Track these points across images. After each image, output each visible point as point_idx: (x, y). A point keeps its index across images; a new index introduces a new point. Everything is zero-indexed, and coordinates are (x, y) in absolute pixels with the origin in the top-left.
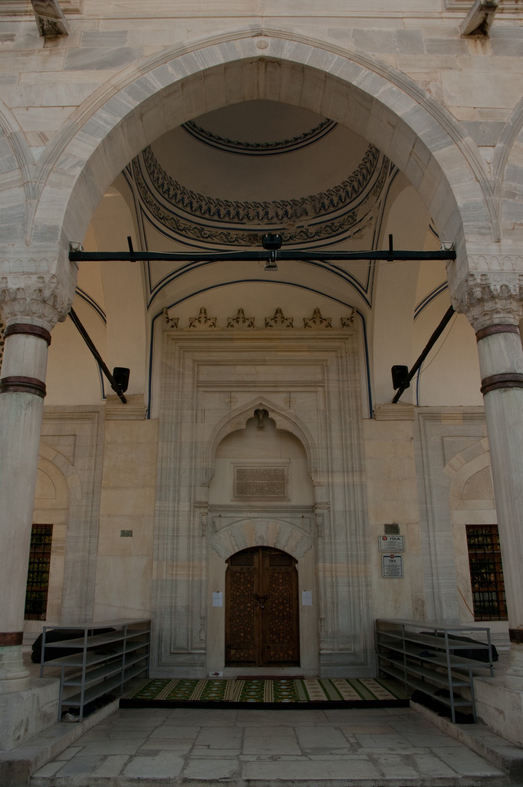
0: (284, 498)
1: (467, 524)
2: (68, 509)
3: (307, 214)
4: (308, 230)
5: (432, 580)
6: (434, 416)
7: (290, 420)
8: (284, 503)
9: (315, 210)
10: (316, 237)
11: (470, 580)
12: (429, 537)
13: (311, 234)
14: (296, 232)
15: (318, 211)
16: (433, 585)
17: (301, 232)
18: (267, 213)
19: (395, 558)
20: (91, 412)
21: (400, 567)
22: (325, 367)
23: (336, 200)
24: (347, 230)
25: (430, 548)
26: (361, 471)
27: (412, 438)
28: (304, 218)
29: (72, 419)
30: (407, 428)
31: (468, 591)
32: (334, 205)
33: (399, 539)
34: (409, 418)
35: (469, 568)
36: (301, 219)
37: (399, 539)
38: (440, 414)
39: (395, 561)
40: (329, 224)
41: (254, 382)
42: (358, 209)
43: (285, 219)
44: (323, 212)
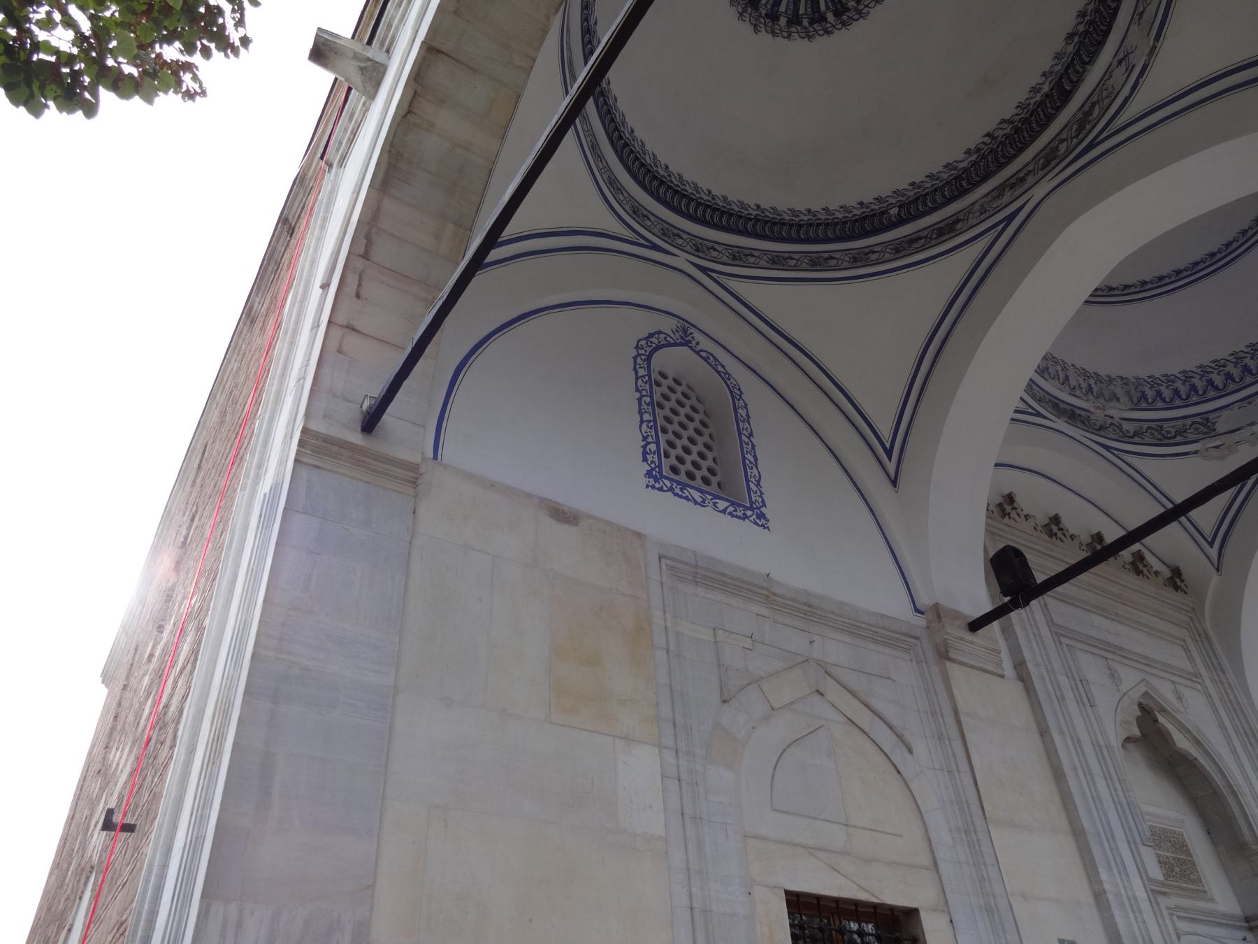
0: (1202, 894)
2: (936, 865)
3: (1118, 400)
7: (1189, 732)
8: (1210, 906)
9: (1131, 399)
15: (1135, 401)
18: (1067, 378)
20: (904, 634)
23: (1167, 393)
24: (1197, 441)
28: (1114, 403)
29: (876, 642)
40: (1153, 425)
41: (1122, 649)
42: (1216, 414)
43: (1091, 397)
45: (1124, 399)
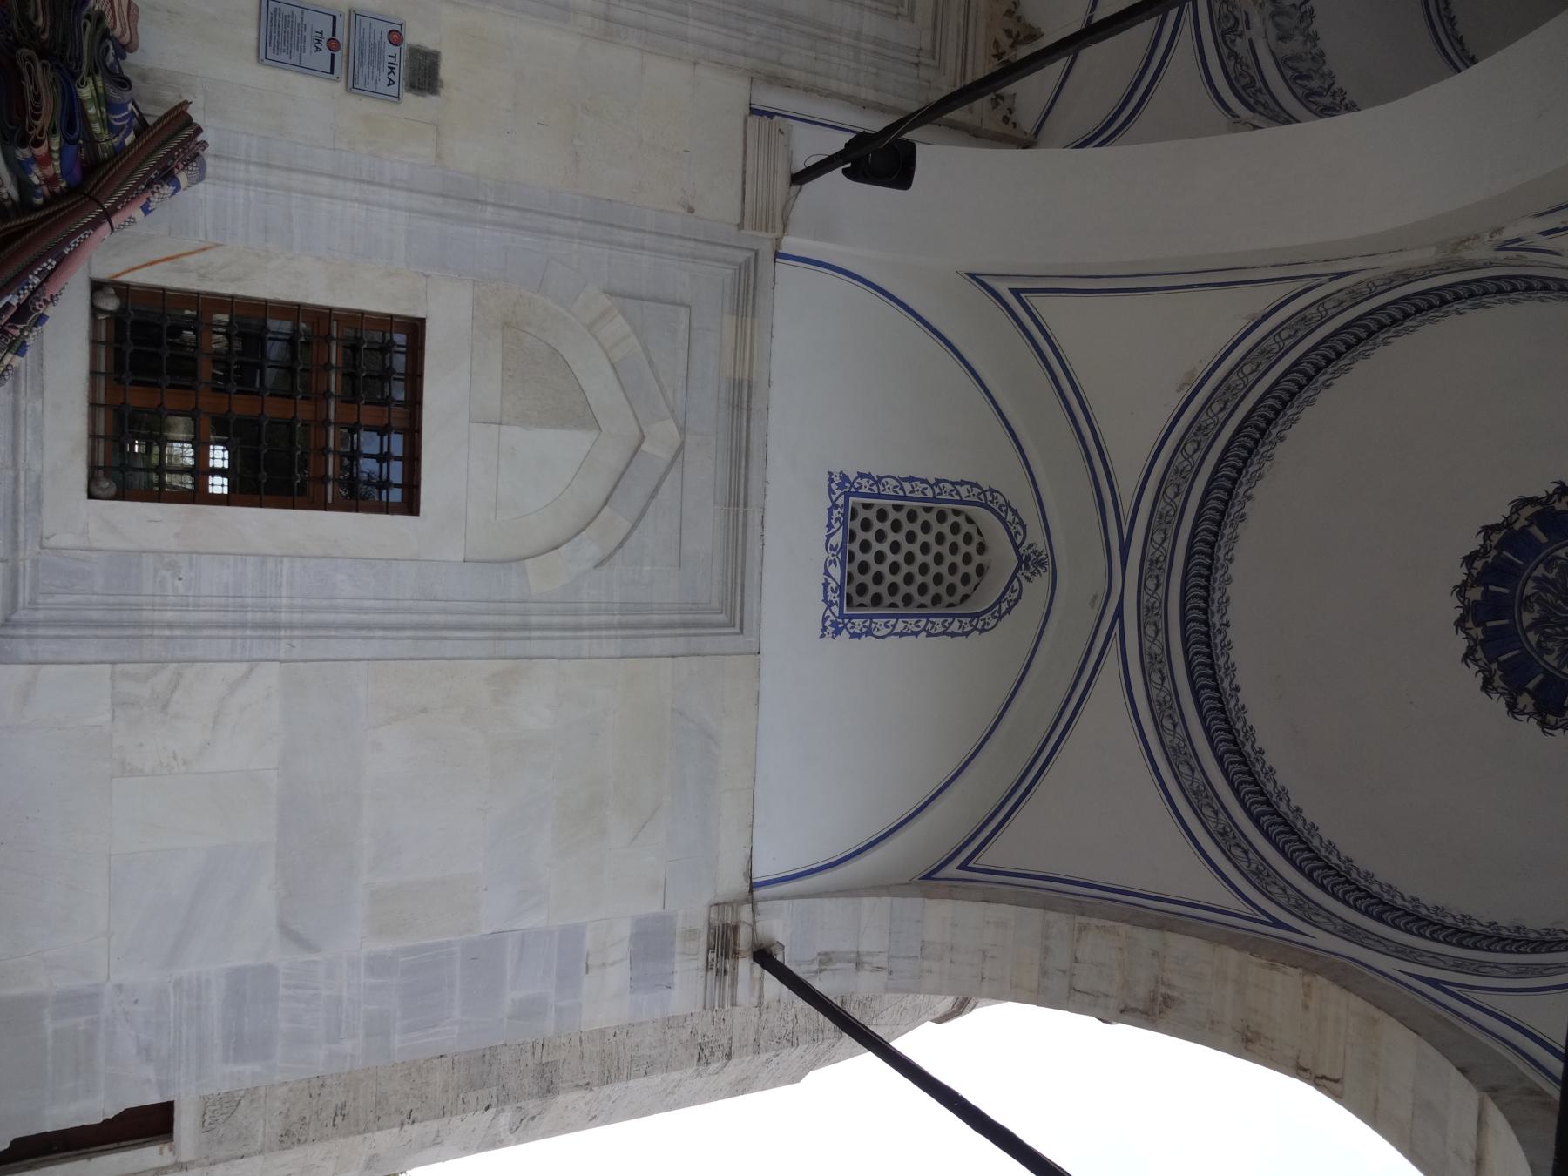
1: (428, 324)
3: (1282, 38)
4: (1241, 36)
5: (248, 163)
6: (747, 294)
9: (1290, 59)
10: (1225, 51)
11: (241, 292)
12: (392, 187)
13: (1233, 41)
14: (1234, 6)
16: (228, 159)
17: (1237, 20)
19: (326, 53)
21: (295, 60)
22: (894, 10)
24: (1253, 110)
25: (356, 180)
26: (607, 19)
27: (691, 210)
28: (1273, 33)
30: (721, 203)
31: (202, 277)
32: (1308, 96)
33: (391, 83)
34: (747, 215)
35: (282, 298)
36: (1269, 23)
37: (391, 83)
38: (753, 316)
39: (318, 49)
40: (1259, 84)
44: (1289, 73)
45: (1287, 48)
